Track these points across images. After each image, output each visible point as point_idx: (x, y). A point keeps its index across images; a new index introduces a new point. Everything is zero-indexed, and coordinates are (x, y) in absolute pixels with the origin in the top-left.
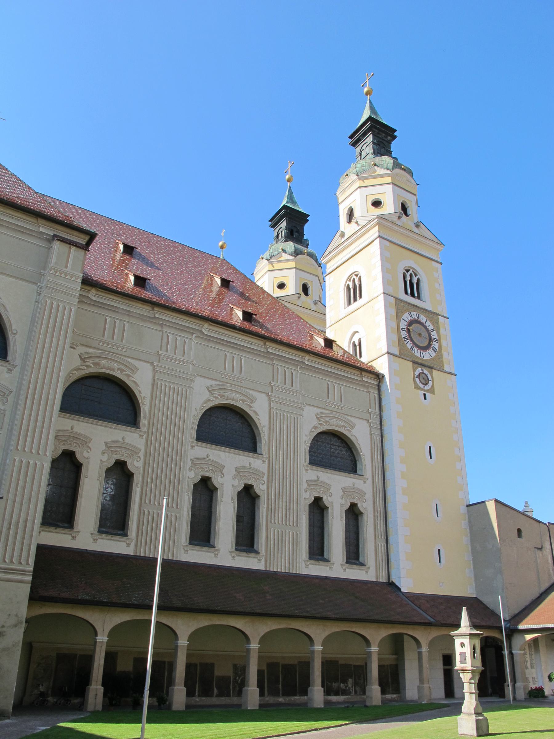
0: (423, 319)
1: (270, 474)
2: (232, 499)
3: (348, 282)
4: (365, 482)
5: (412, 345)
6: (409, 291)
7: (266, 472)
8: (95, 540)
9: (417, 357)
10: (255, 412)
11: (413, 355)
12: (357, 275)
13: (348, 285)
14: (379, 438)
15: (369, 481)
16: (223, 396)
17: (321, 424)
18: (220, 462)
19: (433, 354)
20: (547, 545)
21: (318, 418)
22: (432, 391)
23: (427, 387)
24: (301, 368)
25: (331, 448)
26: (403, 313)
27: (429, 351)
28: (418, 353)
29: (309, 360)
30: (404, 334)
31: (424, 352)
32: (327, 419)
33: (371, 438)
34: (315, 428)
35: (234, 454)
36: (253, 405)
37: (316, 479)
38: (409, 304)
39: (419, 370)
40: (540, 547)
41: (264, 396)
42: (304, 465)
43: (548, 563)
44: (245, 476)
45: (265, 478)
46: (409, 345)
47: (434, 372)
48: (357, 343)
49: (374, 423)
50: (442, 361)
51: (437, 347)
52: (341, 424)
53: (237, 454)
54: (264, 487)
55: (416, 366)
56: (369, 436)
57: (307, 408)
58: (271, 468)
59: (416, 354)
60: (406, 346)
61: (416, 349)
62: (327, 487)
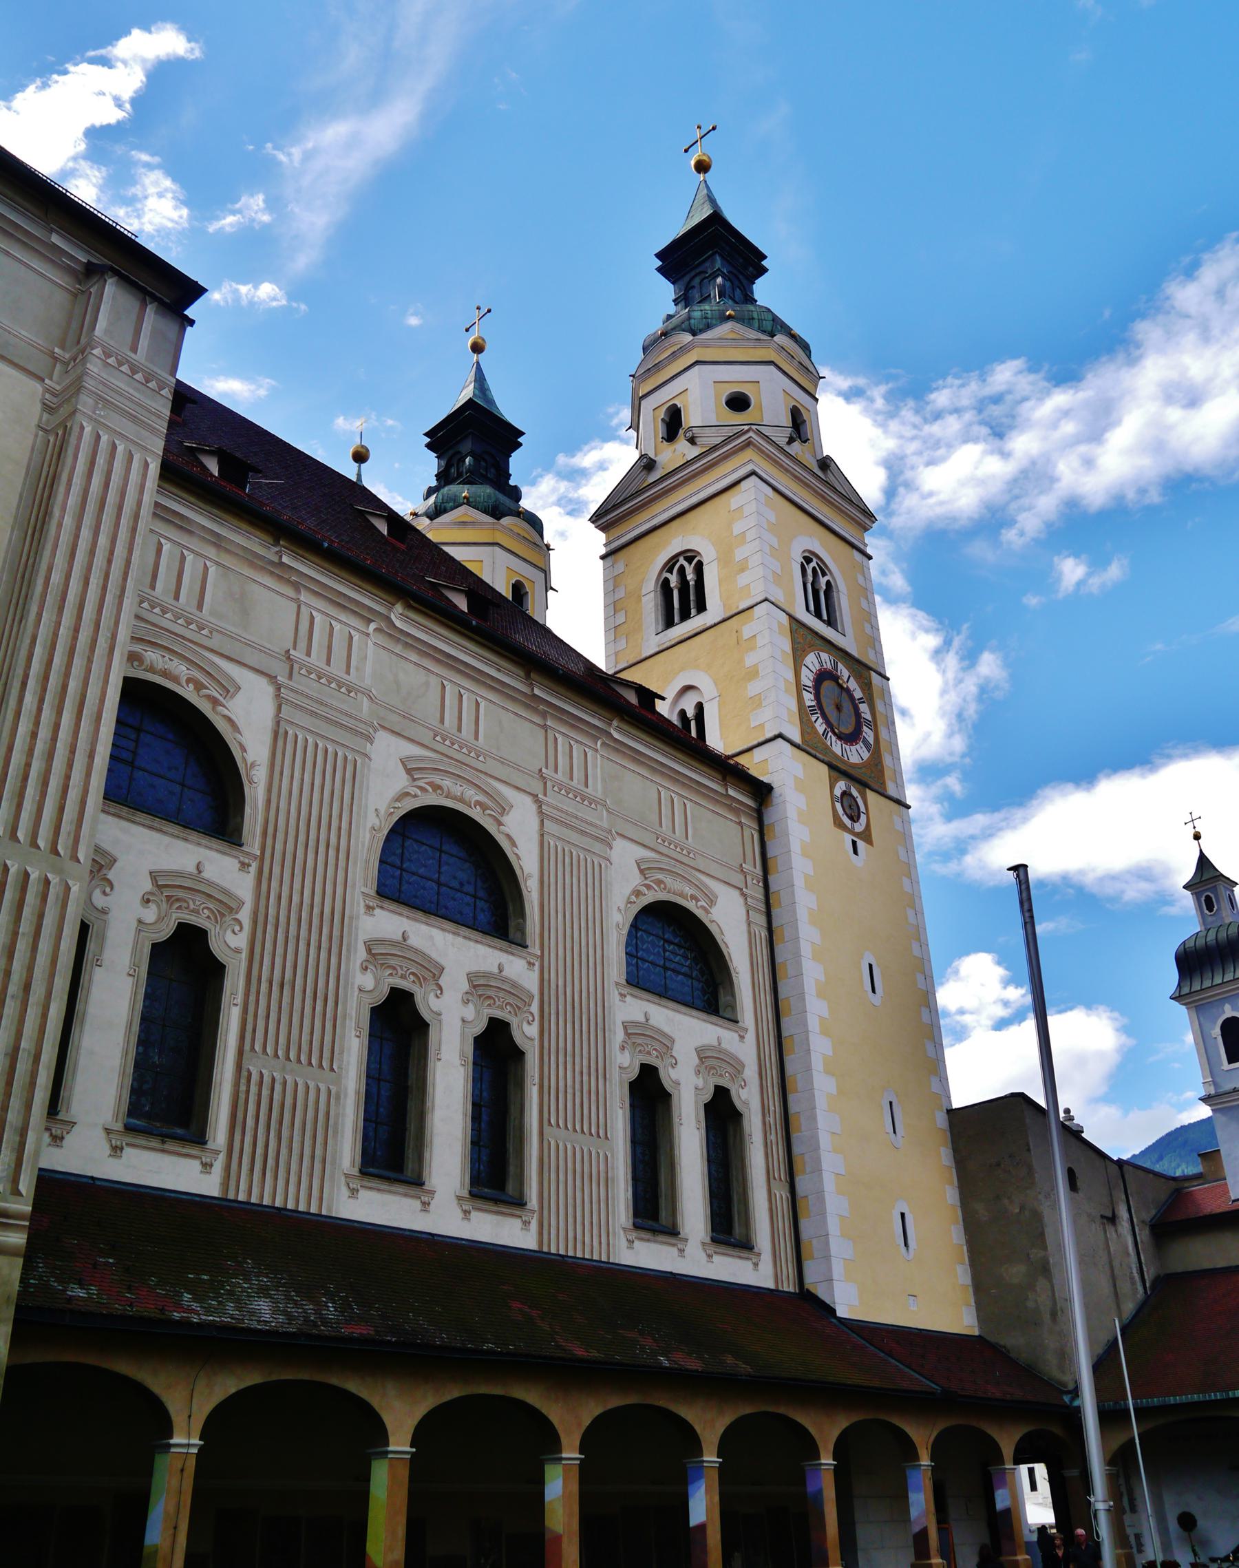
0: (843, 671)
1: (546, 998)
2: (462, 1055)
4: (742, 1037)
7: (534, 988)
8: (117, 1150)
9: (836, 755)
10: (509, 837)
11: (827, 750)
15: (751, 1037)
16: (440, 787)
17: (648, 887)
18: (434, 955)
19: (866, 755)
21: (642, 871)
22: (866, 836)
23: (859, 827)
24: (603, 744)
28: (837, 747)
29: (618, 729)
30: (809, 699)
32: (661, 876)
33: (749, 933)
34: (637, 893)
35: (465, 937)
36: (505, 819)
37: (642, 1019)
38: (816, 633)
39: (841, 786)
41: (528, 800)
42: (617, 984)
44: (489, 997)
45: (535, 1008)
46: (820, 727)
47: (869, 794)
50: (882, 772)
51: (871, 740)
52: (689, 891)
53: (470, 939)
54: (532, 1030)
55: (835, 774)
57: (619, 844)
58: (546, 984)
59: (834, 748)
60: (814, 727)
61: (834, 738)
62: (666, 1044)
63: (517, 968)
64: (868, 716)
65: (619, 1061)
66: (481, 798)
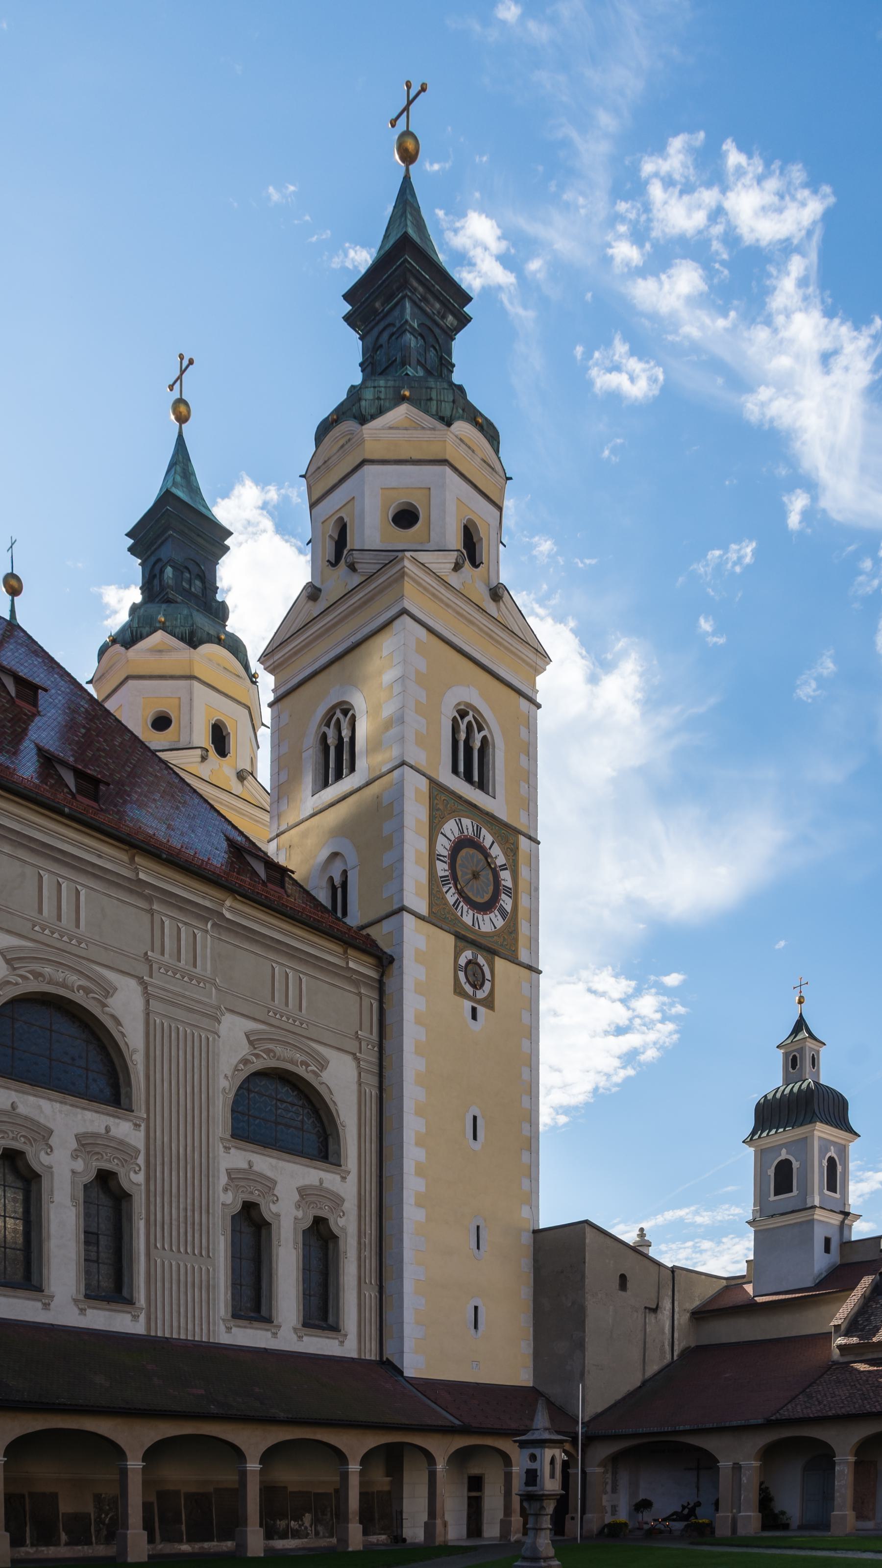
0: (487, 839)
1: (152, 1152)
2: (73, 1198)
3: (325, 729)
4: (344, 1179)
5: (456, 896)
6: (461, 768)
7: (141, 1146)
9: (465, 925)
10: (113, 1017)
11: (458, 920)
12: (345, 712)
13: (324, 737)
14: (375, 1092)
15: (353, 1178)
16: (41, 975)
17: (257, 1056)
18: (42, 1120)
19: (500, 923)
20: (667, 1304)
21: (251, 1043)
22: (489, 1002)
23: (481, 994)
24: (214, 925)
25: (277, 1108)
26: (443, 820)
27: (492, 915)
28: (468, 917)
29: (231, 909)
30: (442, 869)
31: (480, 917)
32: (271, 1046)
33: (360, 1092)
34: (245, 1061)
35: (72, 1105)
36: (110, 1001)
37: (246, 1166)
38: (460, 798)
39: (467, 955)
40: (654, 1307)
41: (133, 983)
42: (221, 1139)
43: (663, 1333)
44: (98, 1153)
45: (141, 1160)
46: (451, 897)
47: (499, 963)
48: (337, 881)
49: (365, 1061)
50: (516, 940)
51: (508, 908)
52: (299, 1057)
53: (77, 1107)
54: (139, 1178)
55: (461, 944)
56: (355, 1087)
57: (228, 1020)
58: (152, 1141)
60: (444, 898)
61: (465, 908)
62: (269, 1185)
63: (123, 1129)
64: (509, 883)
65: (221, 1200)
66: (83, 982)
